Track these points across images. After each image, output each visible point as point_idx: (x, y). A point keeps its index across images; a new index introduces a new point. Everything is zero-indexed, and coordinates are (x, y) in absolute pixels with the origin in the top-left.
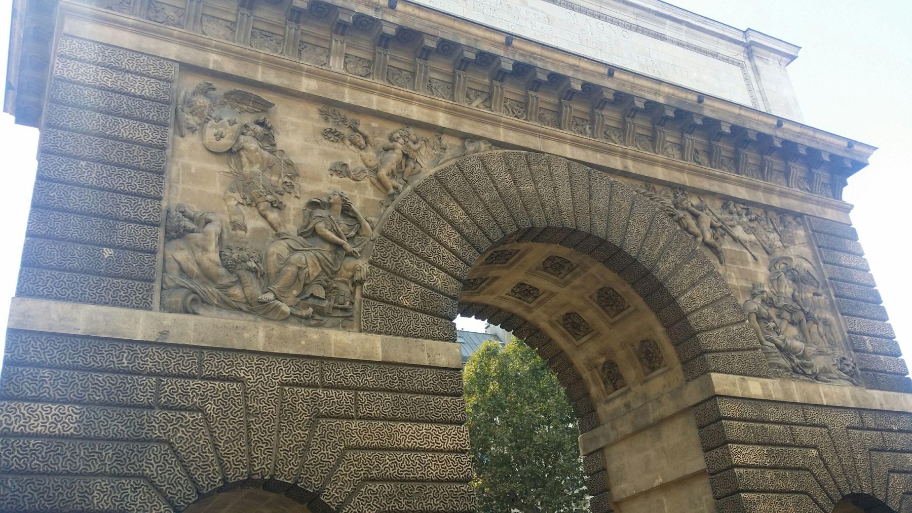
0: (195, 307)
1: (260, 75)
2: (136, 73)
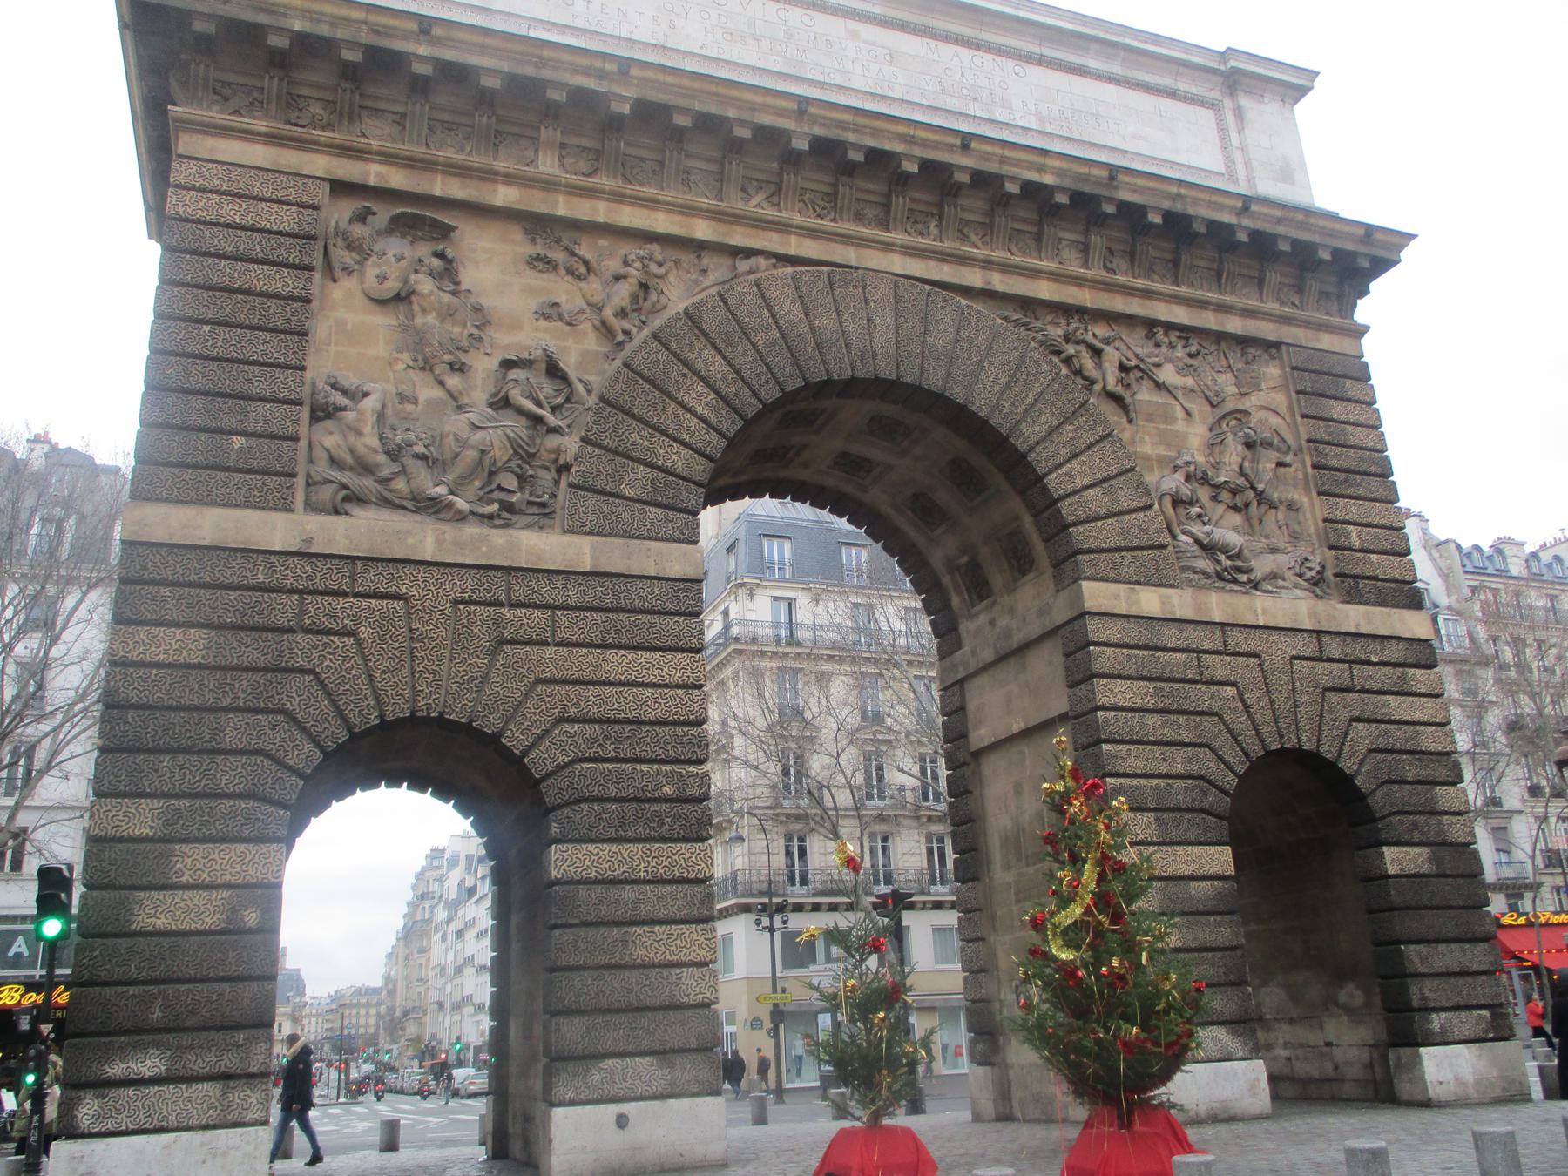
0: (348, 506)
1: (440, 187)
2: (272, 201)
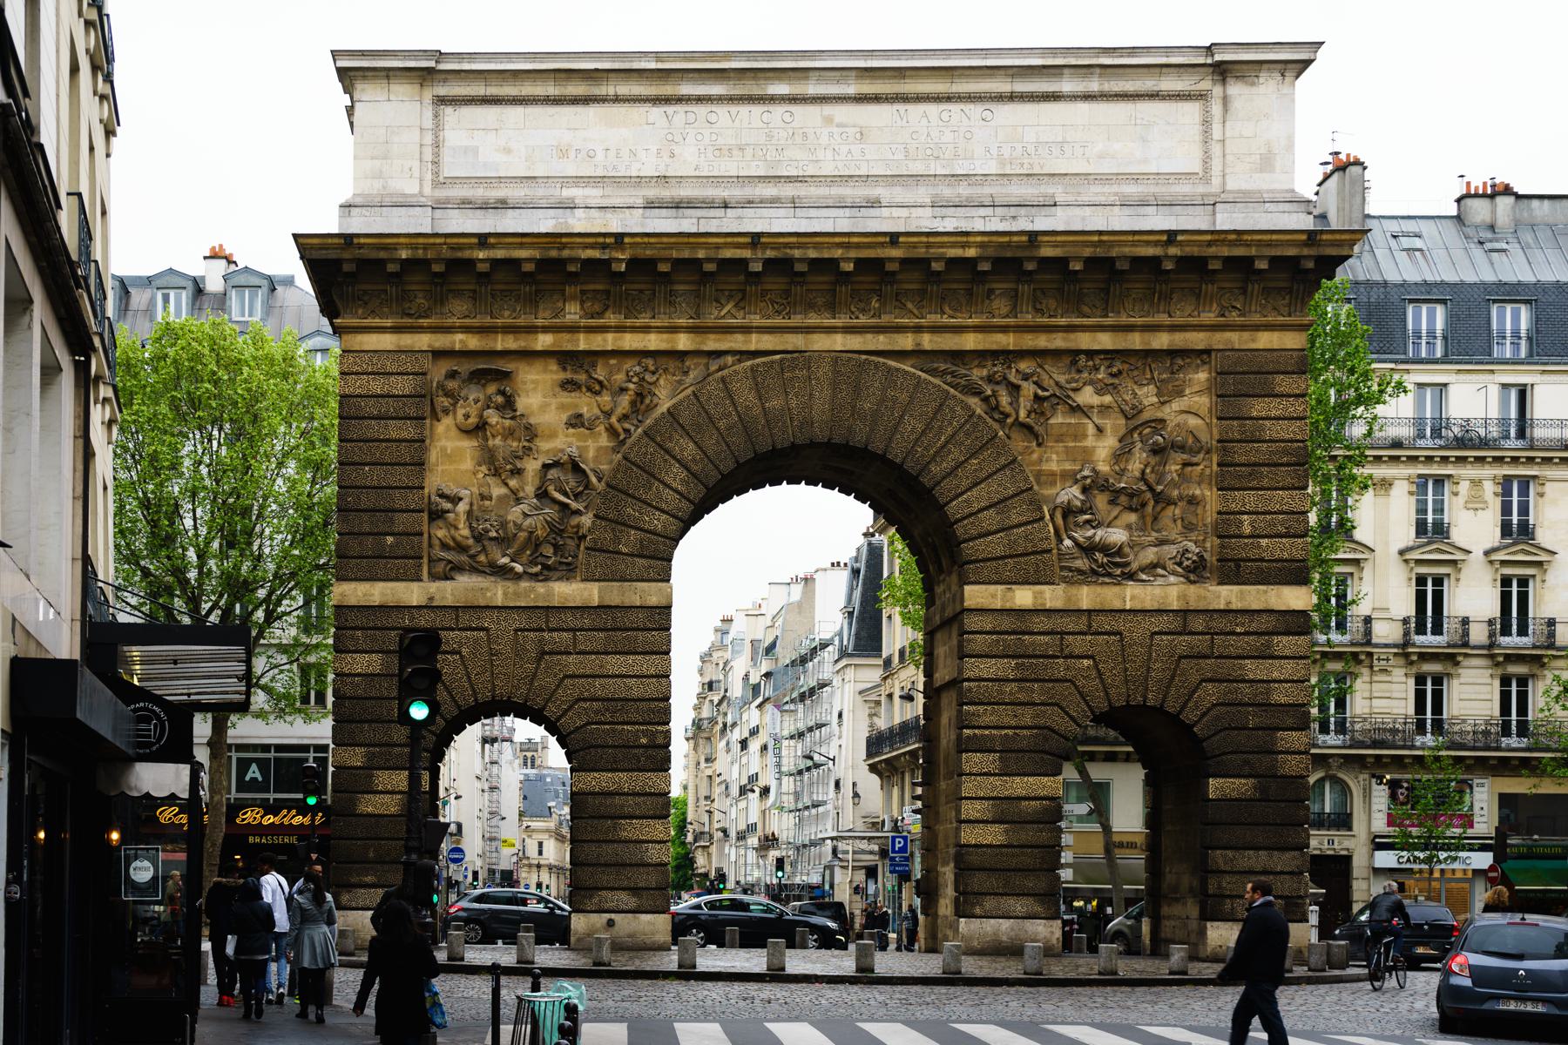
1: (502, 343)
